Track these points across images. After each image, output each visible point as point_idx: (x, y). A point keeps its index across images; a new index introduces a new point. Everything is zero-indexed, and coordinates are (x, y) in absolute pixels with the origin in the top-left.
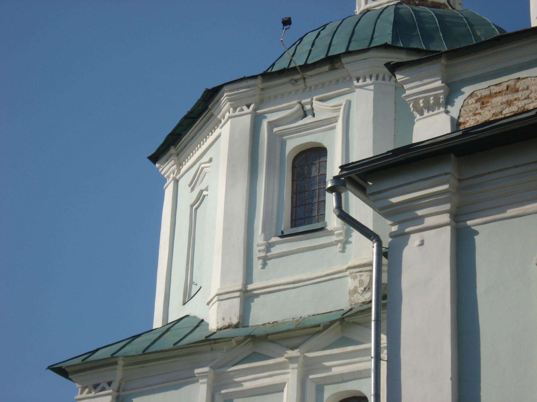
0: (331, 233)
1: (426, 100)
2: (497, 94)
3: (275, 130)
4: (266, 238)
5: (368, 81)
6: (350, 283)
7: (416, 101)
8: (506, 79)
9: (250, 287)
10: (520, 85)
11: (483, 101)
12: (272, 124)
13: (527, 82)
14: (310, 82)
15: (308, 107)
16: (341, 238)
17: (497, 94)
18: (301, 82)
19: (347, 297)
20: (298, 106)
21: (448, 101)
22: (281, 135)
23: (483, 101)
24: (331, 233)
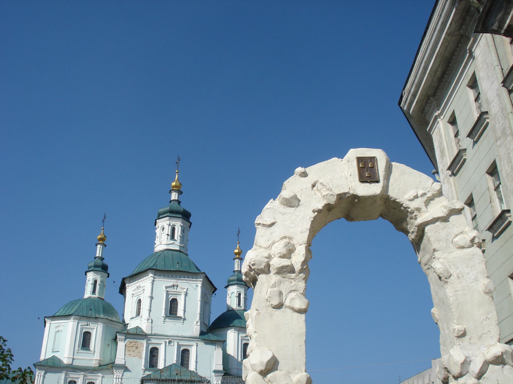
0: (91, 351)
1: (121, 339)
2: (133, 342)
3: (82, 327)
4: (78, 349)
5: (102, 323)
6: (94, 362)
7: (119, 339)
8: (135, 340)
9: (74, 357)
10: (137, 342)
11: (131, 343)
12: (81, 325)
13: (139, 342)
14: (90, 320)
15: (89, 324)
16: (93, 353)
17: (133, 342)
18: (89, 319)
19: (94, 365)
20: (87, 323)
21: (125, 341)
22: (83, 328)
23: (131, 343)
24: (91, 351)
